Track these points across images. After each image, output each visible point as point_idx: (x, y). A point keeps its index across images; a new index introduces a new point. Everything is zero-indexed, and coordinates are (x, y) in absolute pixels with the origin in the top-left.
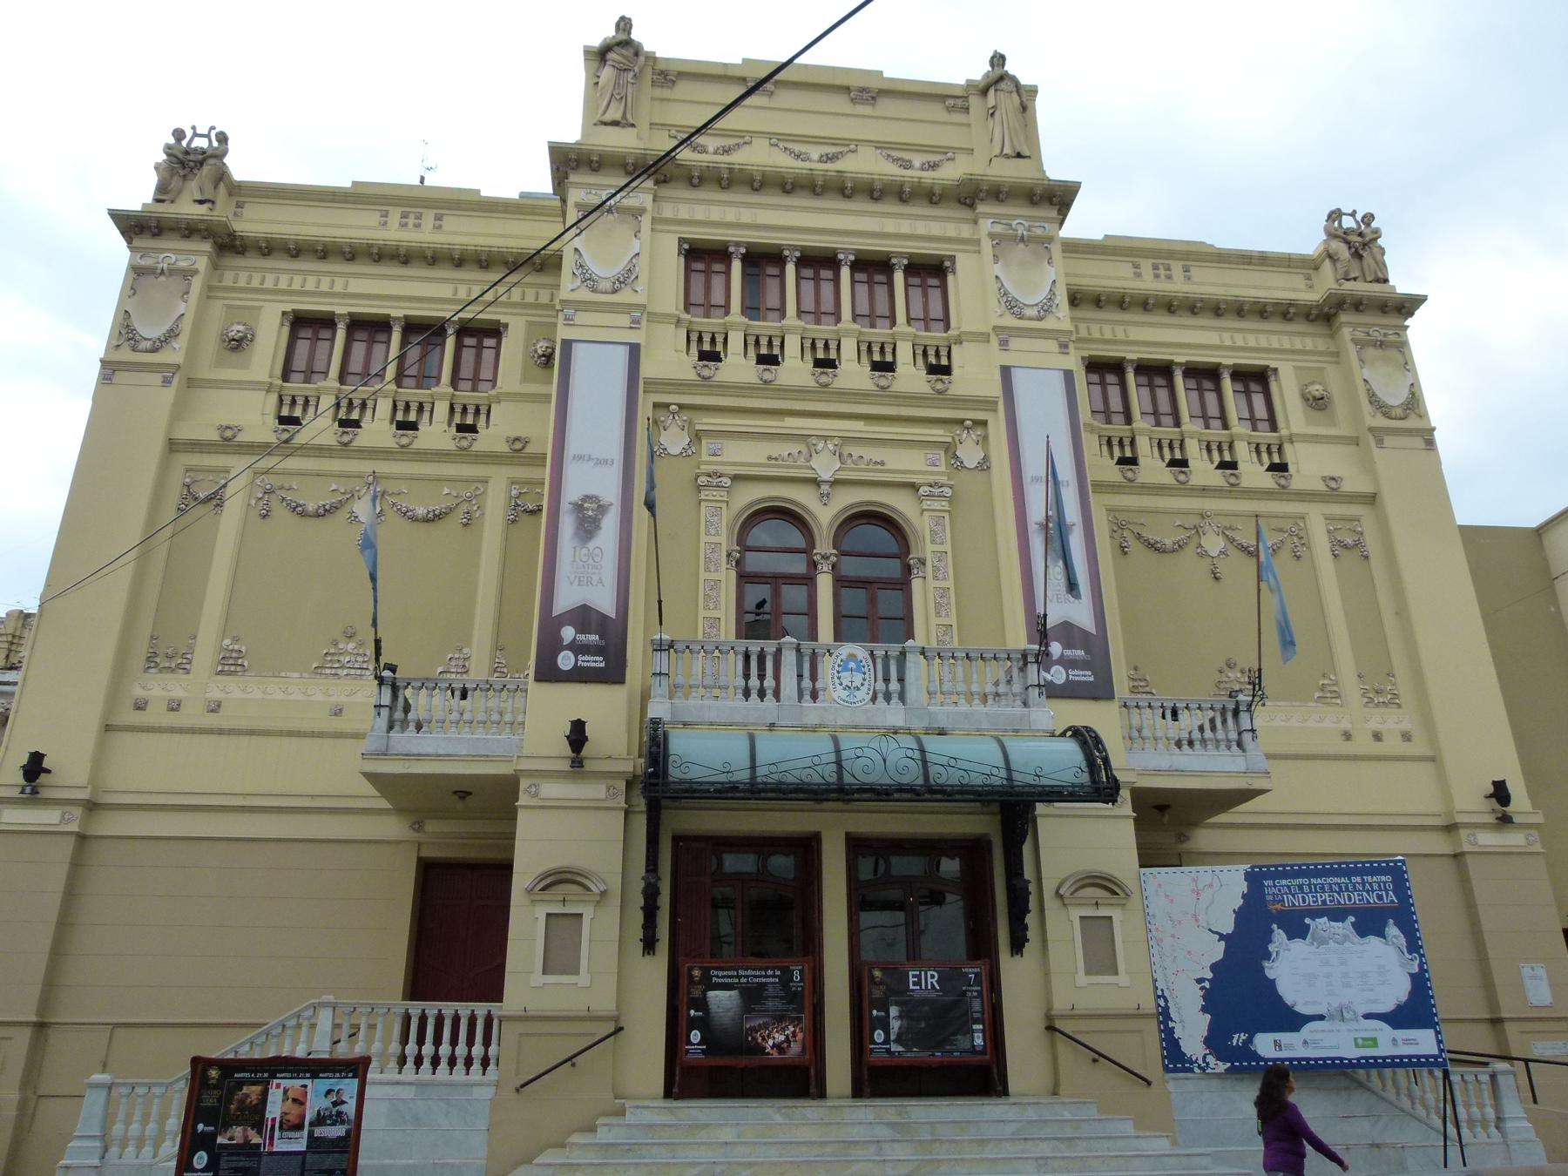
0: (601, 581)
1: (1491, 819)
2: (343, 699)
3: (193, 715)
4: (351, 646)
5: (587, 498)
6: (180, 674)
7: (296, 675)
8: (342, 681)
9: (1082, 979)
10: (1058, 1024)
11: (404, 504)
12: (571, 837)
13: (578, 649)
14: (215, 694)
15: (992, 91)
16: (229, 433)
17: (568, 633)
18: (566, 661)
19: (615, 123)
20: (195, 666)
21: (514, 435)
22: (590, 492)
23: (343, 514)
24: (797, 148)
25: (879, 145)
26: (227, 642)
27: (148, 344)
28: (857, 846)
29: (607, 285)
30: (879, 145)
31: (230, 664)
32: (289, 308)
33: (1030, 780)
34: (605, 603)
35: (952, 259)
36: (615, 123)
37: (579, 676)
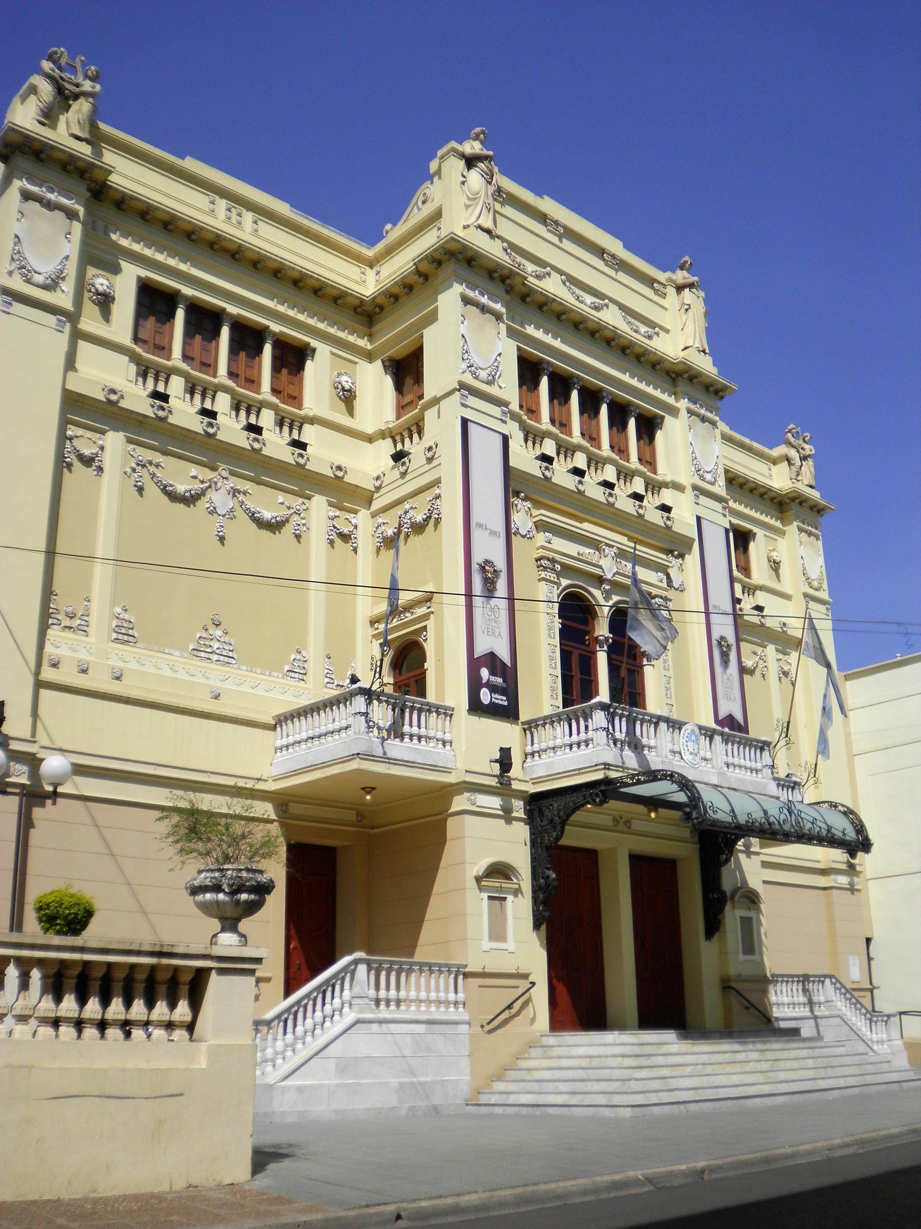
0: (500, 634)
1: (844, 867)
2: (219, 684)
3: (99, 681)
4: (218, 633)
5: (487, 562)
6: (79, 637)
7: (177, 653)
8: (213, 666)
9: (741, 957)
10: (732, 984)
11: (249, 504)
12: (490, 839)
13: (493, 689)
14: (116, 662)
15: (687, 290)
16: (114, 397)
17: (485, 673)
18: (485, 696)
19: (488, 232)
20: (92, 630)
21: (337, 463)
22: (489, 558)
23: (203, 504)
24: (578, 292)
25: (622, 308)
26: (118, 610)
27: (39, 279)
28: (637, 861)
29: (483, 375)
30: (622, 308)
31: (124, 634)
32: (144, 273)
33: (840, 835)
34: (504, 655)
35: (662, 418)
36: (488, 232)
37: (493, 711)
